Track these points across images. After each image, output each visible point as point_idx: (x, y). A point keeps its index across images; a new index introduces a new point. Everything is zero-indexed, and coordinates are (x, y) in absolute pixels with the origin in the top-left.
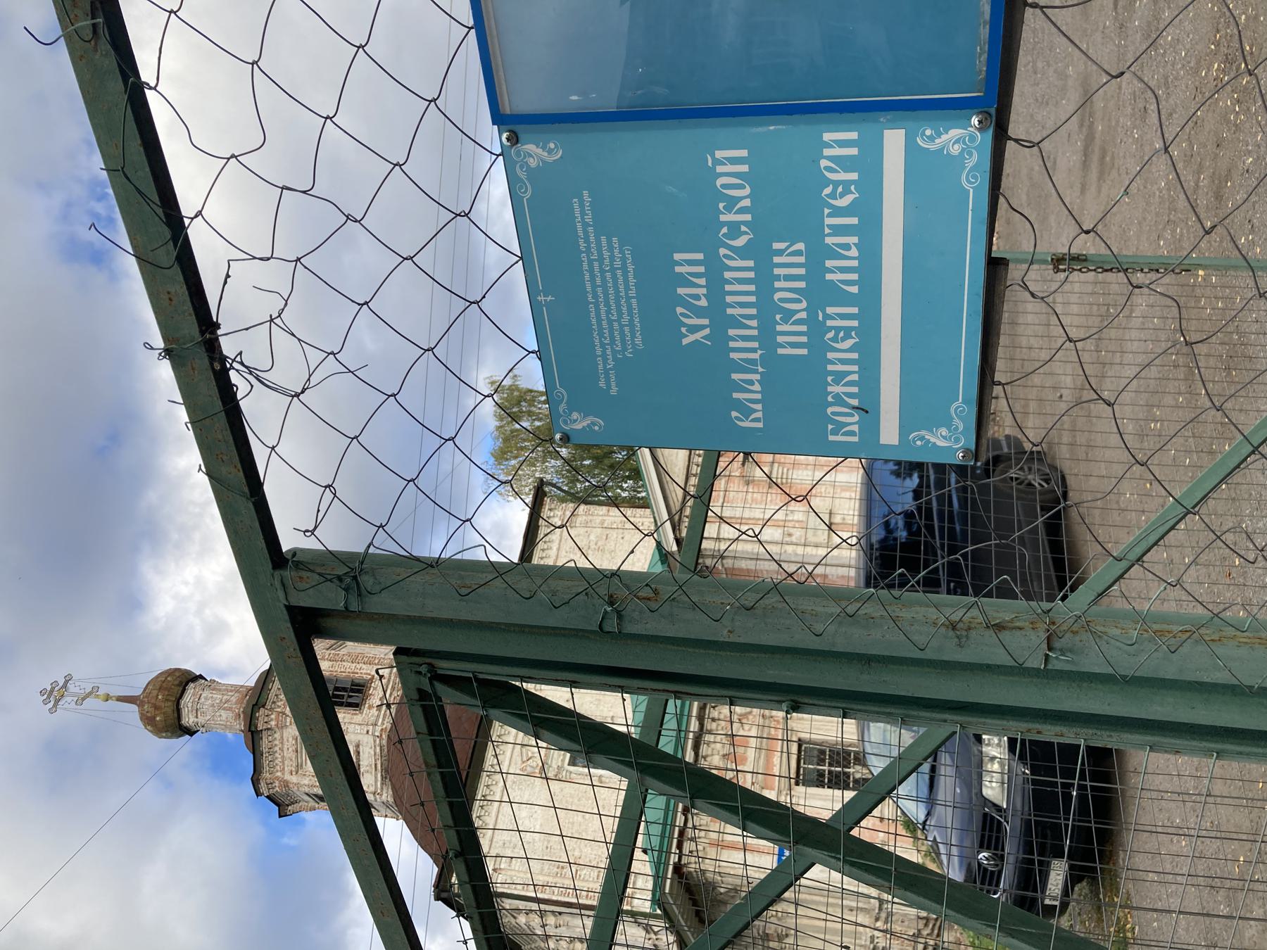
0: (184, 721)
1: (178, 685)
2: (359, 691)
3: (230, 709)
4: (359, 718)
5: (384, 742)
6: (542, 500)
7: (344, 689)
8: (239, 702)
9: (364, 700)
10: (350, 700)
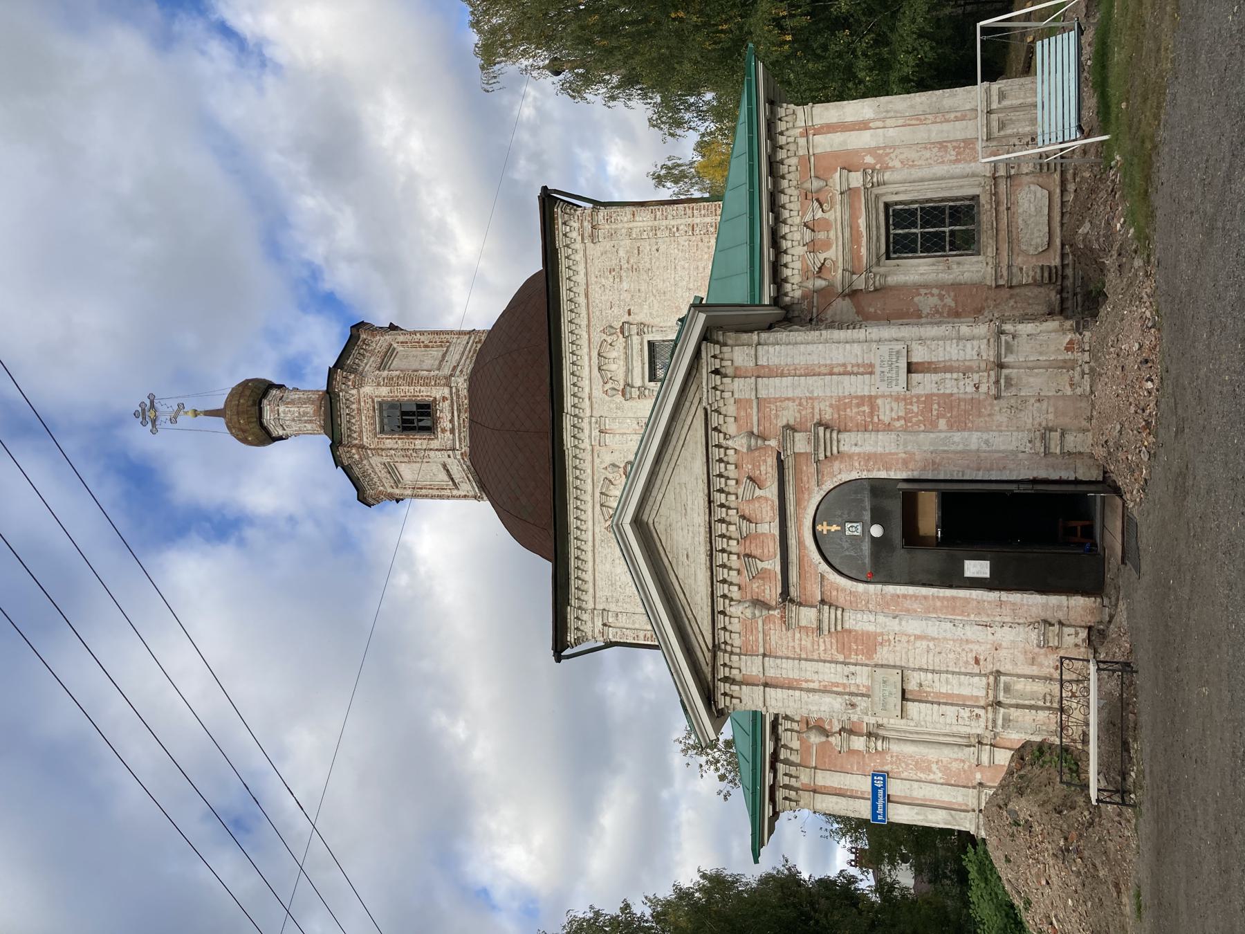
0: (275, 434)
1: (254, 404)
2: (428, 414)
3: (310, 422)
4: (435, 444)
5: (469, 463)
6: (552, 213)
7: (413, 414)
8: (317, 412)
9: (435, 421)
10: (421, 424)
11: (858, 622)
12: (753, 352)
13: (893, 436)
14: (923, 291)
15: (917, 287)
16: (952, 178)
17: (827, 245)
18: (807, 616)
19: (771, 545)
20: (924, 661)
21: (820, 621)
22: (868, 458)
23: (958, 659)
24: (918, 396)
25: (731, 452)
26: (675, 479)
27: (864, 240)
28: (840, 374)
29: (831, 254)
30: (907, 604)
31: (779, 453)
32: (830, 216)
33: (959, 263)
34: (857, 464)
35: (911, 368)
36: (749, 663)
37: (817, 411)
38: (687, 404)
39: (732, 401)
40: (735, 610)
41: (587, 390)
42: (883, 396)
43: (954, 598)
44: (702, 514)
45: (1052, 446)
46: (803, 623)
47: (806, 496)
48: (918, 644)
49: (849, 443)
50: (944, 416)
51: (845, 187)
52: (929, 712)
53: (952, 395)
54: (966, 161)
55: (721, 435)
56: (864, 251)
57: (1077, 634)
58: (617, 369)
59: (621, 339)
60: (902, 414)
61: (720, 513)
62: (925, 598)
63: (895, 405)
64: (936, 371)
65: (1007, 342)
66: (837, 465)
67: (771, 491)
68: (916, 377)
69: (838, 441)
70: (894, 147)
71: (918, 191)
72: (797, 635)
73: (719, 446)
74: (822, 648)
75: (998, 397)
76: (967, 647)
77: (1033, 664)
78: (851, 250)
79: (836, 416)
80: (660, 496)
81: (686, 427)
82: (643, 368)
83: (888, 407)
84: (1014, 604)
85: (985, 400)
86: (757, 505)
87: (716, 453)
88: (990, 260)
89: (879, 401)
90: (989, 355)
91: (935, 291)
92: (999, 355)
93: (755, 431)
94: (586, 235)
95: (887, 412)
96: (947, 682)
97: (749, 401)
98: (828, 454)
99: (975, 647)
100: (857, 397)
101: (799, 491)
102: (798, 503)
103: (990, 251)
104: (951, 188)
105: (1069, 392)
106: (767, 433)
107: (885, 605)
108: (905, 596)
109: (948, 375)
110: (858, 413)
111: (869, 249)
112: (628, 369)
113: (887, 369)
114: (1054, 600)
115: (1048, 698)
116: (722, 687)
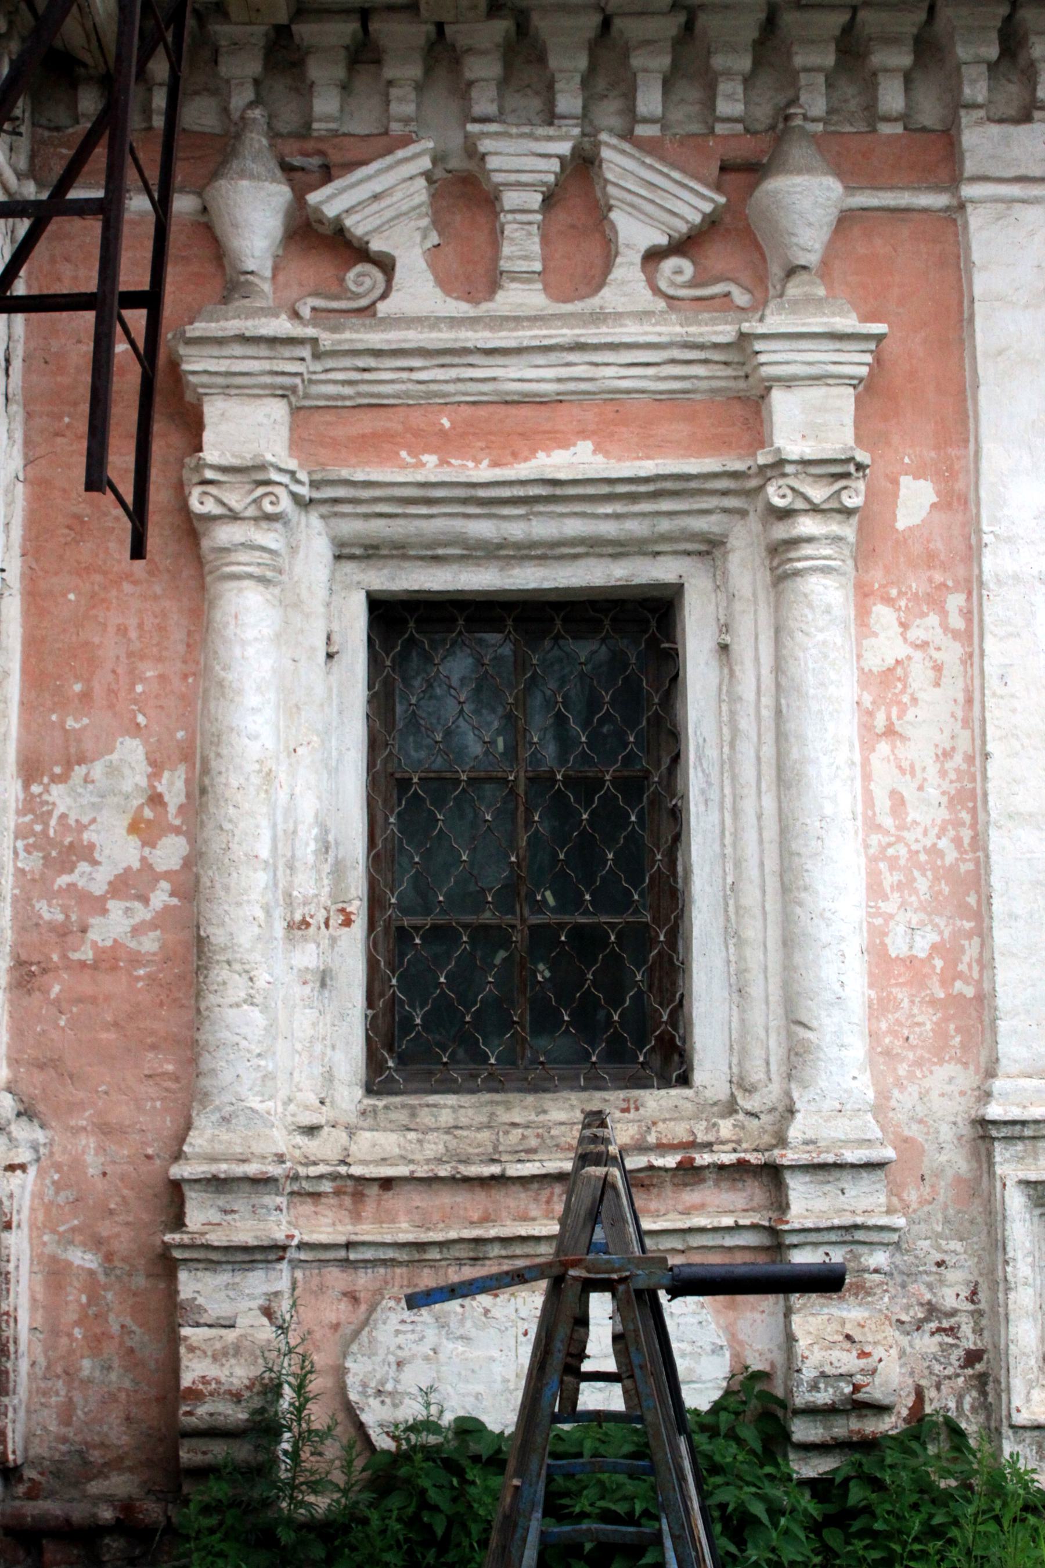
14: (174, 787)
15: (194, 757)
16: (790, 942)
17: (476, 275)
27: (483, 472)
32: (626, 286)
33: (324, 979)
51: (774, 359)
54: (878, 1008)
70: (971, 634)
71: (730, 765)
78: (433, 400)
88: (326, 1148)
91: (169, 853)
103: (383, 1145)
104: (732, 935)
111: (425, 497)
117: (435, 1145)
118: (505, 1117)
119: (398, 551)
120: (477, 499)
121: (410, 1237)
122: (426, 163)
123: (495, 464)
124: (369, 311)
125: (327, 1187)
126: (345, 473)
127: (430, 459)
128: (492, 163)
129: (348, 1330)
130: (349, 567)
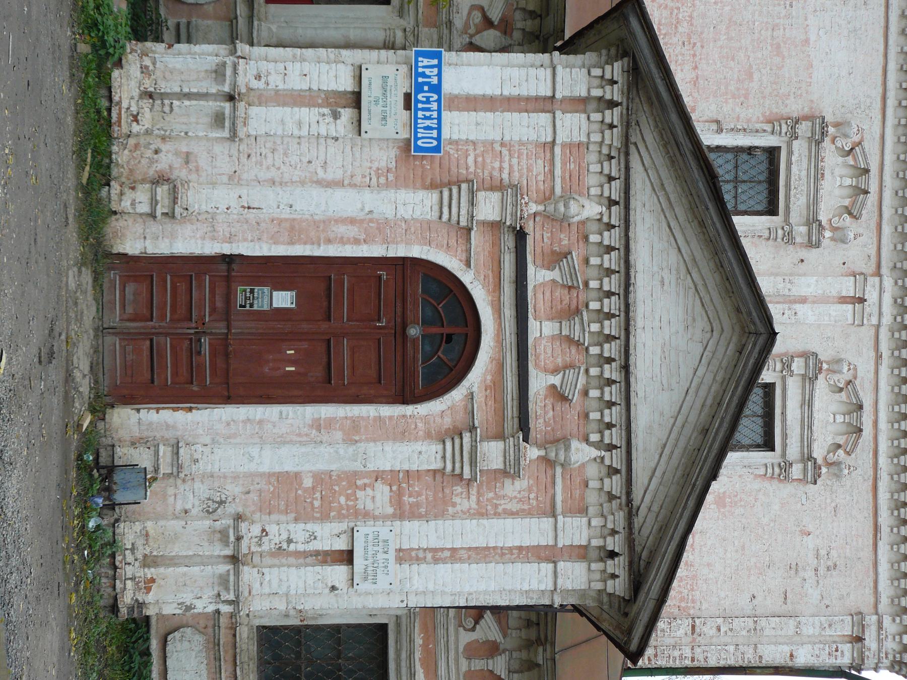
11: (419, 204)
12: (560, 582)
13: (371, 467)
17: (472, 651)
18: (489, 208)
19: (540, 305)
20: (331, 150)
21: (472, 203)
22: (402, 434)
23: (286, 154)
24: (340, 517)
25: (595, 437)
26: (677, 396)
27: (418, 655)
28: (442, 550)
29: (466, 638)
30: (351, 231)
31: (526, 439)
33: (287, 616)
34: (420, 425)
35: (348, 557)
36: (575, 133)
37: (474, 498)
38: (655, 508)
39: (591, 510)
40: (592, 210)
41: (884, 371)
42: (385, 518)
43: (291, 243)
44: (639, 346)
45: (169, 454)
46: (495, 196)
47: (489, 377)
48: (339, 175)
49: (425, 455)
50: (306, 490)
52: (324, 77)
53: (296, 520)
55: (607, 462)
56: (419, 641)
57: (133, 204)
58: (827, 406)
59: (818, 453)
60: (360, 494)
61: (611, 349)
62: (329, 241)
63: (370, 506)
64: (317, 553)
65: (227, 589)
66: (447, 422)
67: (538, 383)
68: (341, 545)
69: (444, 457)
72: (505, 176)
73: (611, 447)
74: (471, 160)
75: (239, 518)
76: (273, 173)
77: (188, 154)
79: (447, 491)
80: (700, 373)
81: (658, 473)
82: (784, 406)
83: (378, 503)
84: (213, 239)
85: (254, 512)
86: (559, 361)
87: (614, 436)
89: (390, 510)
90: (248, 574)
92: (237, 574)
93: (559, 470)
94: (874, 628)
95: (379, 498)
96: (300, 124)
97: (570, 512)
98: (457, 441)
99: (263, 175)
100: (420, 517)
101: (496, 386)
102: (501, 366)
103: (244, 632)
105: (149, 524)
106: (543, 467)
107: (383, 228)
108: (357, 242)
109: (301, 547)
110: (419, 494)
111: (411, 641)
112: (810, 405)
113: (381, 556)
114: (163, 248)
115: (167, 109)
116: (615, 93)
117: (244, 647)
118: (251, 663)
119: (398, 632)
120: (411, 654)
121: (221, 642)
122: (498, 641)
123: (420, 659)
124: (460, 625)
125: (234, 620)
126: (417, 620)
127: (421, 642)
128: (499, 657)
129: (197, 626)
130: (395, 619)
